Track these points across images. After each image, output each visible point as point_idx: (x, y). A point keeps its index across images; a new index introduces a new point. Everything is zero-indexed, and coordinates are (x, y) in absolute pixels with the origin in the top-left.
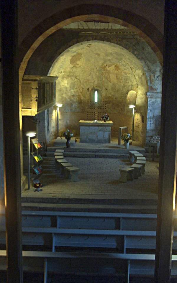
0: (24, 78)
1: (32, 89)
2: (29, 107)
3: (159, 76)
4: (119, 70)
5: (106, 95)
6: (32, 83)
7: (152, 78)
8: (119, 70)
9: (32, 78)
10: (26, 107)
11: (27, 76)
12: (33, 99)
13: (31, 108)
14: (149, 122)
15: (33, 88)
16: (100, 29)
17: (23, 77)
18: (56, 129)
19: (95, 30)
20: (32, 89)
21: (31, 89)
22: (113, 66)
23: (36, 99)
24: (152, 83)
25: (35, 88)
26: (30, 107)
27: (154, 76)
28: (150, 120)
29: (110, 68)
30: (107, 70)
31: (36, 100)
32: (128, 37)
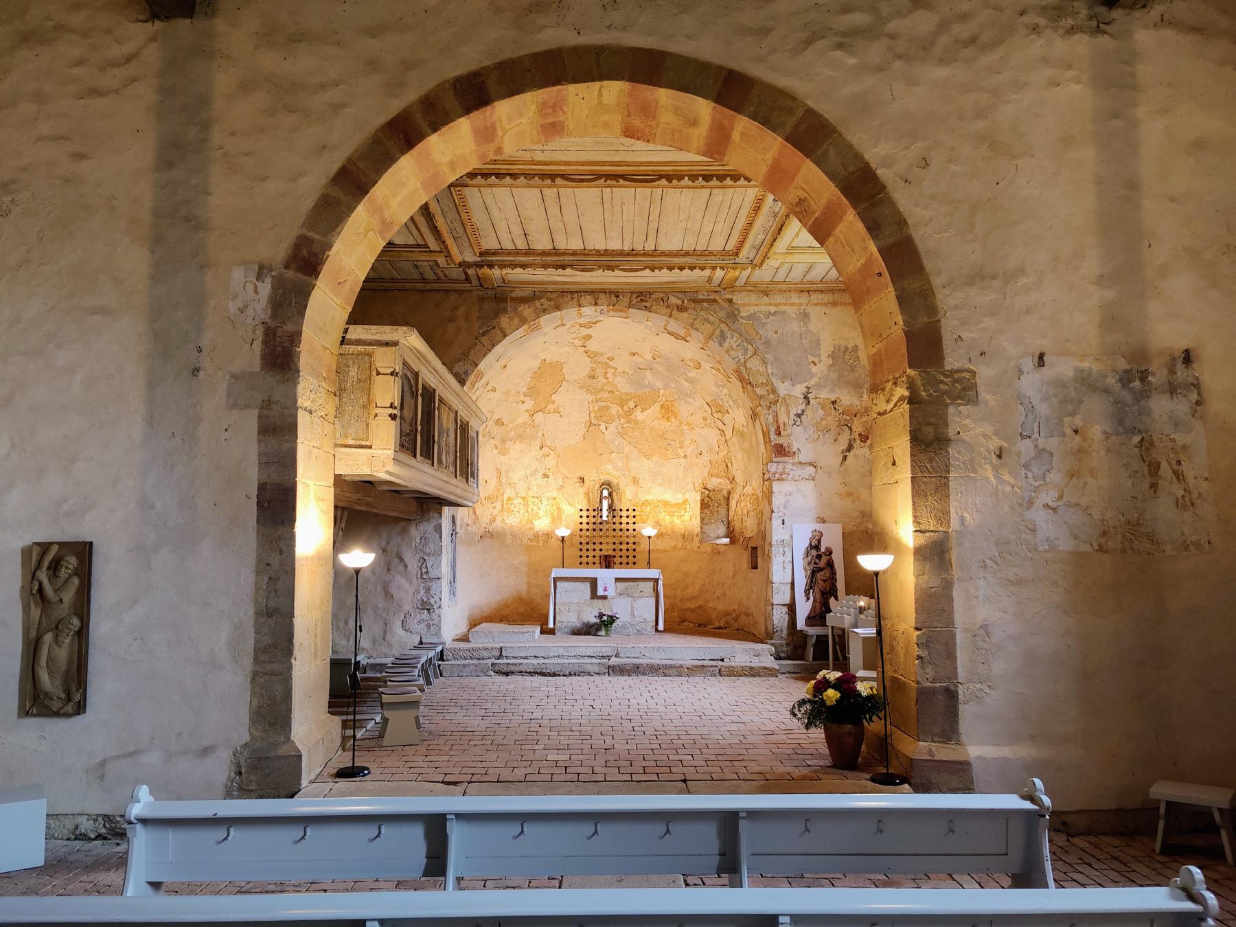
0: (348, 336)
1: (378, 373)
2: (363, 443)
3: (803, 411)
4: (673, 419)
5: (636, 495)
6: (379, 352)
7: (783, 418)
8: (673, 419)
9: (377, 337)
10: (352, 442)
11: (359, 328)
12: (377, 410)
13: (370, 447)
14: (782, 558)
15: (381, 371)
16: (621, 253)
17: (346, 331)
18: (405, 280)
19: (606, 253)
20: (378, 373)
21: (374, 373)
22: (657, 407)
23: (391, 411)
24: (783, 433)
25: (389, 371)
26: (368, 443)
27: (788, 413)
28: (781, 549)
29: (646, 413)
30: (636, 422)
31: (393, 417)
32: (701, 297)
